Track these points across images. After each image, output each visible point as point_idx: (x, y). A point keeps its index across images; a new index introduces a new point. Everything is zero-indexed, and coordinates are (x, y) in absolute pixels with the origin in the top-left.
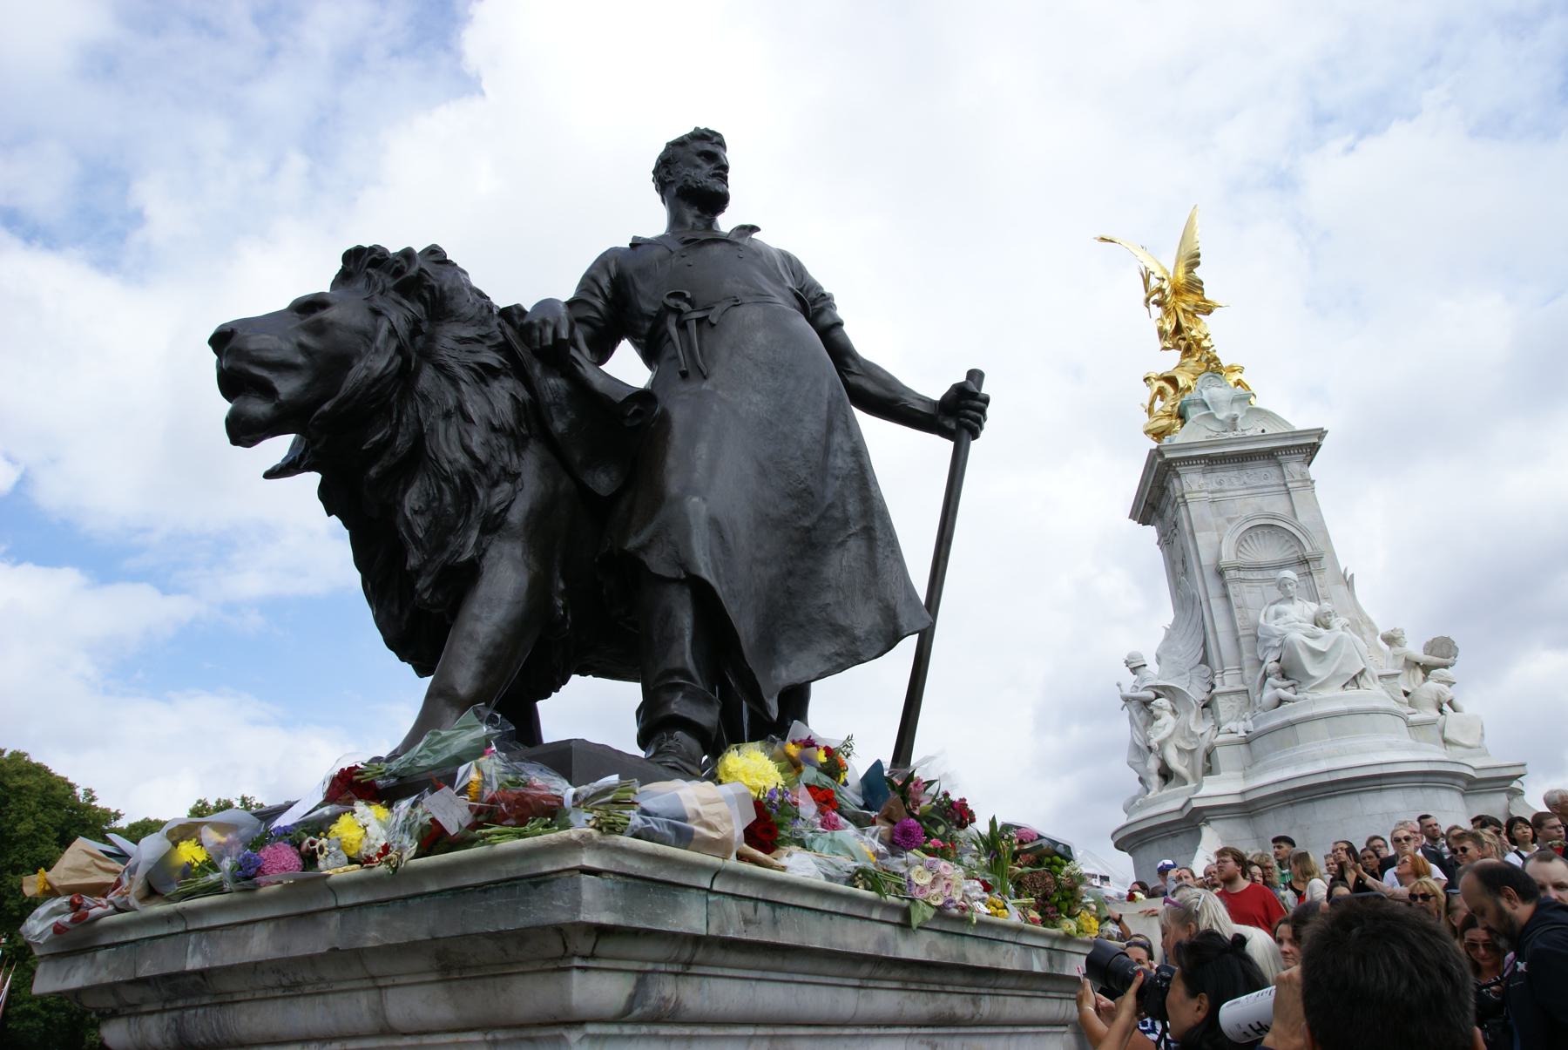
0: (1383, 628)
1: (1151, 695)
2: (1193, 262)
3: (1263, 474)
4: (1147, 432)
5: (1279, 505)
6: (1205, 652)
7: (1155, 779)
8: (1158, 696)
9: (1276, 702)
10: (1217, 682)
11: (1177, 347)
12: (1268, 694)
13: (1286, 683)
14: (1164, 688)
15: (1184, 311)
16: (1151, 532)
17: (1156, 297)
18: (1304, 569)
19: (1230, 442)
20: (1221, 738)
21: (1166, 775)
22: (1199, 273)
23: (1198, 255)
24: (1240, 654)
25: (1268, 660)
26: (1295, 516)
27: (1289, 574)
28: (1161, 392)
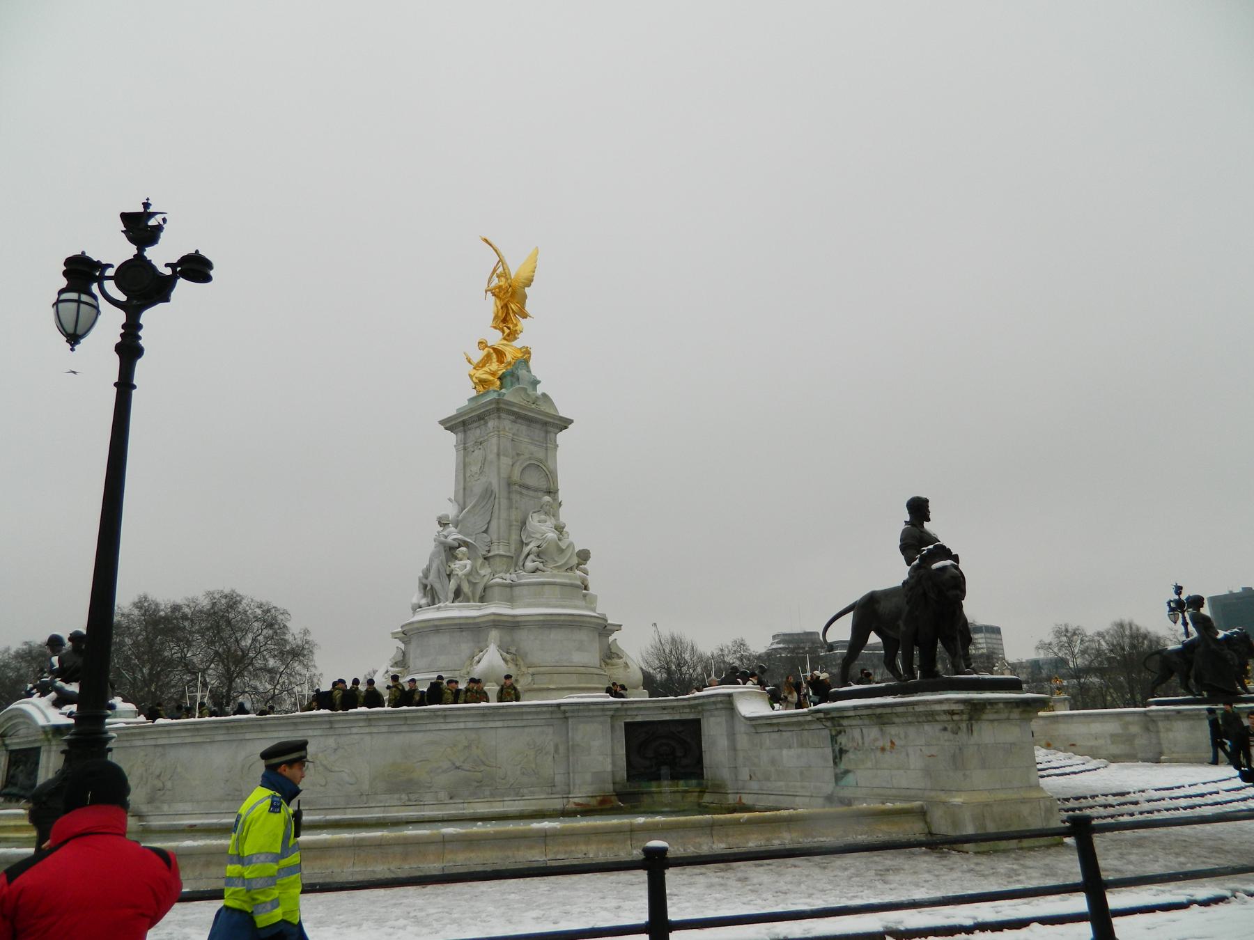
2: (529, 282)
3: (538, 433)
5: (540, 454)
8: (460, 546)
12: (529, 565)
19: (531, 410)
24: (510, 534)
28: (488, 356)
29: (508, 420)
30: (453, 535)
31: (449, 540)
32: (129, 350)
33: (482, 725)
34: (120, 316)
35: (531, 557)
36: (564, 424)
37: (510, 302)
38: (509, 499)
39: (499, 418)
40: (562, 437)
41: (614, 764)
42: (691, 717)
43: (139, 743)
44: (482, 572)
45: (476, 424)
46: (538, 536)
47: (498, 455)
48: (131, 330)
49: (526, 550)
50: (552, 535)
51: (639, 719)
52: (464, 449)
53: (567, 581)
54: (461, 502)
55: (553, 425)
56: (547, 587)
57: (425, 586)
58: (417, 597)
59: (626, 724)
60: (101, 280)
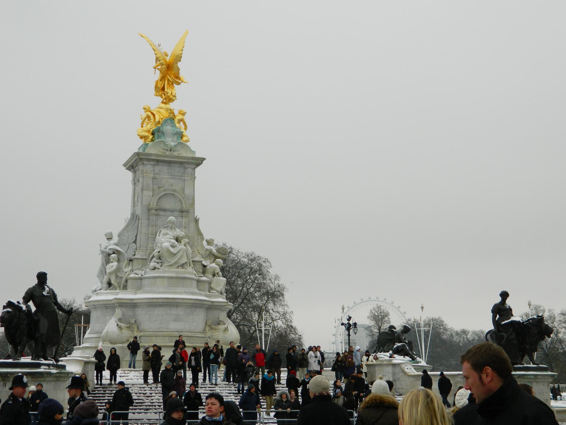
0: (207, 236)
1: (112, 252)
2: (178, 58)
3: (177, 170)
4: (138, 135)
6: (136, 239)
7: (105, 285)
8: (114, 253)
9: (153, 268)
10: (137, 253)
11: (161, 96)
12: (152, 264)
13: (159, 261)
14: (117, 251)
15: (168, 80)
16: (130, 174)
17: (159, 67)
18: (180, 214)
19: (167, 156)
20: (132, 275)
21: (110, 284)
23: (181, 57)
25: (156, 251)
26: (183, 190)
27: (172, 218)
28: (148, 117)
29: (164, 163)
35: (154, 259)
36: (199, 162)
39: (143, 164)
40: (199, 170)
44: (125, 270)
47: (142, 190)
53: (174, 275)
55: (189, 163)
56: (159, 280)
58: (97, 284)
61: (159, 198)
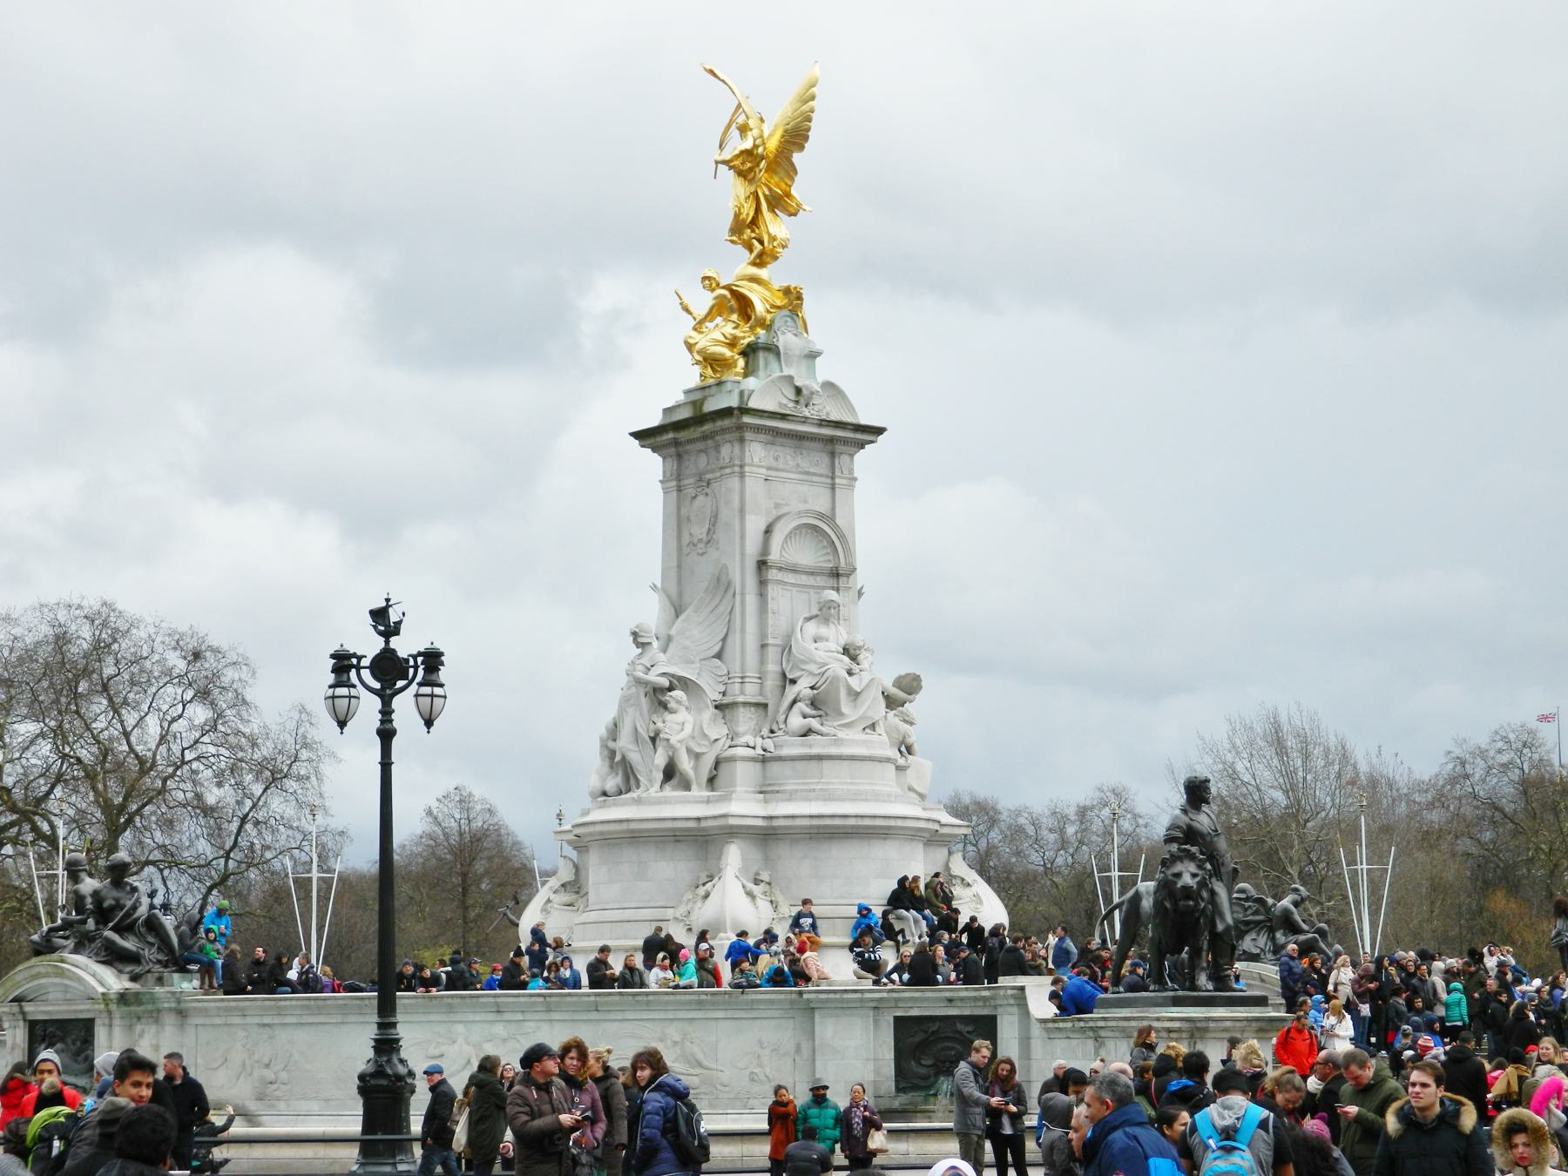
3: (815, 461)
12: (796, 721)
14: (681, 679)
22: (797, 158)
30: (663, 666)
31: (653, 677)
32: (386, 735)
33: (700, 1014)
34: (377, 703)
37: (767, 170)
38: (762, 595)
40: (865, 460)
41: (877, 1072)
42: (986, 1012)
43: (237, 1020)
45: (700, 445)
46: (812, 667)
48: (386, 713)
49: (791, 692)
50: (839, 666)
51: (915, 1013)
52: (676, 482)
54: (673, 590)
55: (846, 441)
56: (826, 764)
57: (613, 753)
59: (896, 1018)
60: (358, 668)
61: (785, 541)
